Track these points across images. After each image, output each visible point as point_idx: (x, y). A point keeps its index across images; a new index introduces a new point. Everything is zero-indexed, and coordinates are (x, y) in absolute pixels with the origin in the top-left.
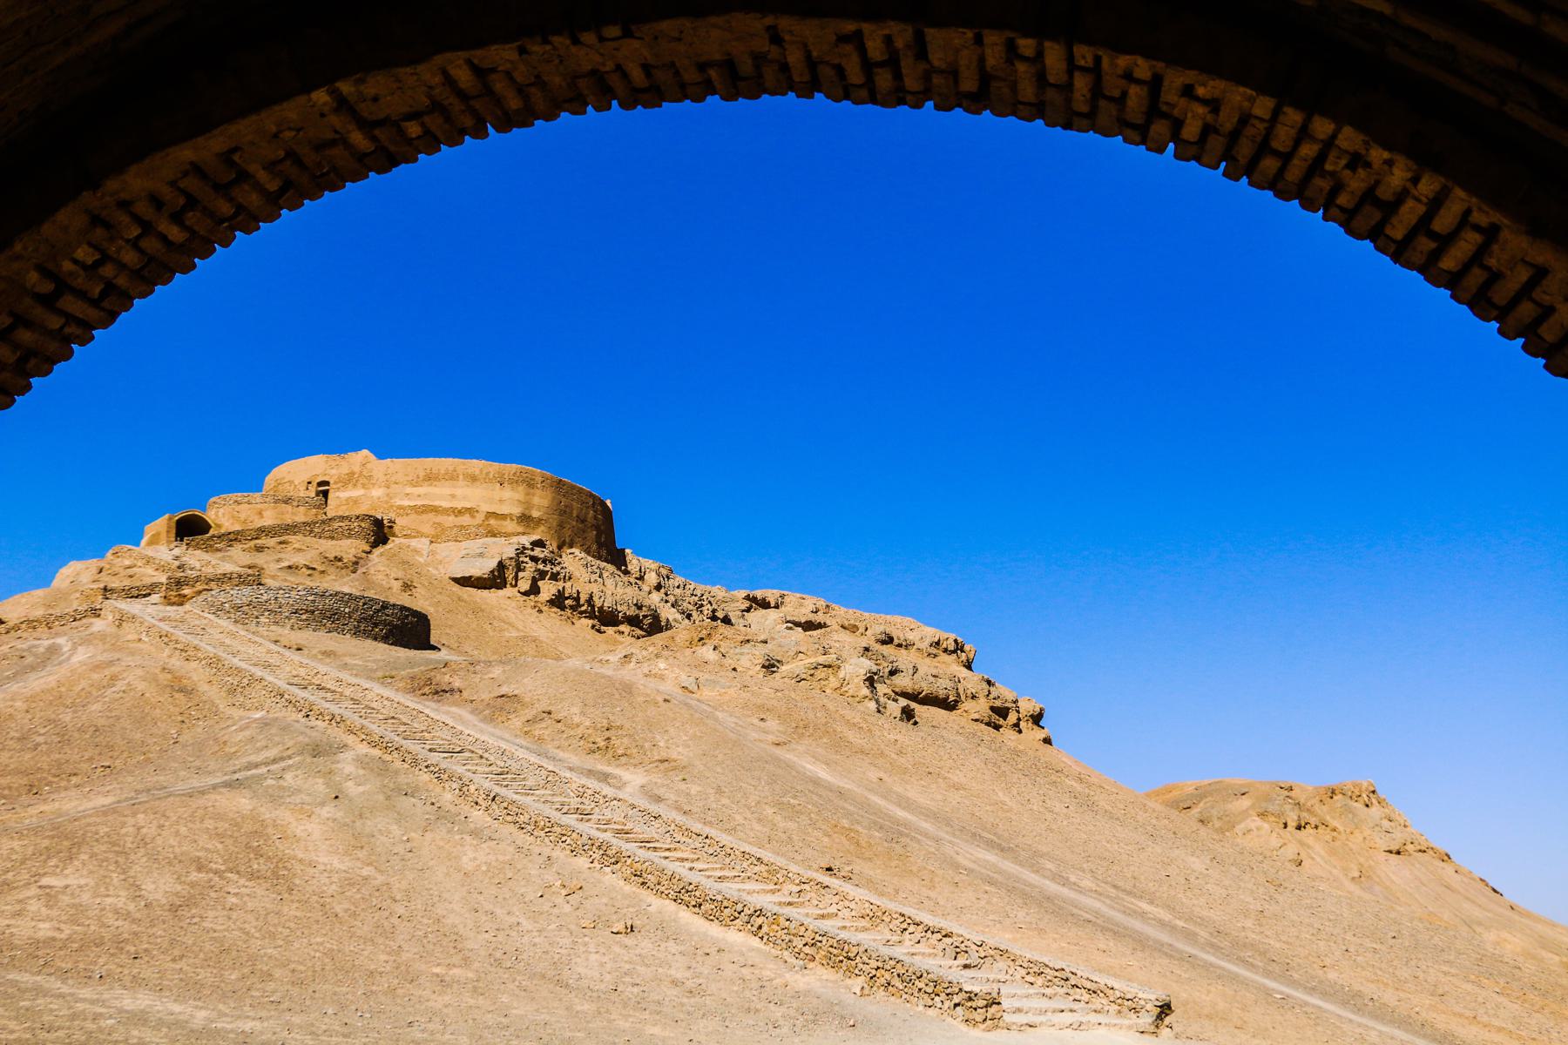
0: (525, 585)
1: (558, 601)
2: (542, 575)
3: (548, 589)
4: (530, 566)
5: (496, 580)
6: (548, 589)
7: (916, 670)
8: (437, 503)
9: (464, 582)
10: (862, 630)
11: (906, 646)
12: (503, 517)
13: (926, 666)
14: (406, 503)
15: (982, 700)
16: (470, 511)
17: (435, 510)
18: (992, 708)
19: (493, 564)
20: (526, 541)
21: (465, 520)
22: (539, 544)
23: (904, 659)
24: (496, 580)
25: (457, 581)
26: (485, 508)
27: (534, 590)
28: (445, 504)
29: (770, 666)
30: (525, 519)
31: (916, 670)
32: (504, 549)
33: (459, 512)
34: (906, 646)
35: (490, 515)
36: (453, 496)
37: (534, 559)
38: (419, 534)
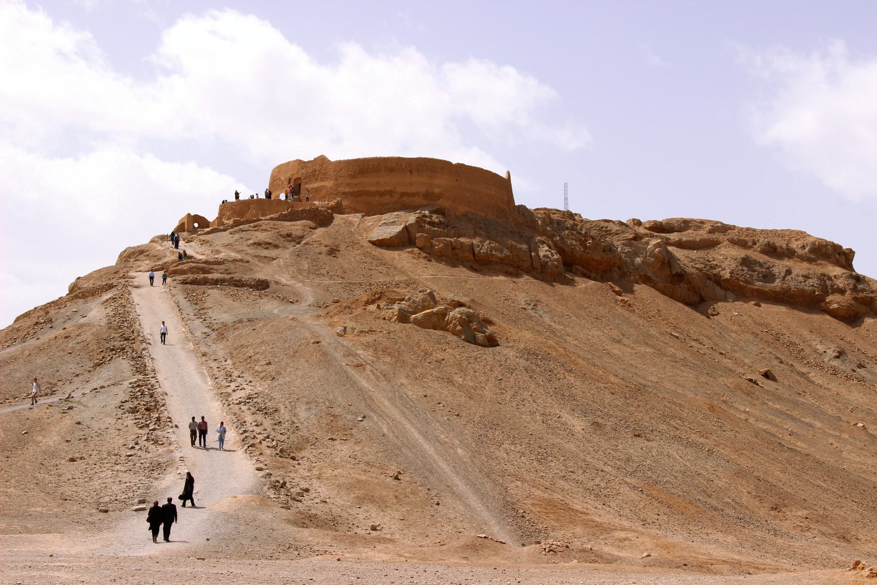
7: (789, 272)
8: (367, 189)
9: (381, 244)
10: (750, 244)
11: (789, 253)
12: (413, 195)
13: (799, 268)
14: (347, 190)
15: (848, 292)
16: (391, 193)
17: (368, 193)
18: (855, 299)
19: (399, 228)
21: (387, 199)
23: (779, 266)
25: (374, 243)
26: (399, 189)
28: (373, 189)
31: (789, 272)
33: (382, 194)
34: (789, 253)
35: (403, 194)
36: (378, 183)
37: (430, 223)
38: (356, 211)
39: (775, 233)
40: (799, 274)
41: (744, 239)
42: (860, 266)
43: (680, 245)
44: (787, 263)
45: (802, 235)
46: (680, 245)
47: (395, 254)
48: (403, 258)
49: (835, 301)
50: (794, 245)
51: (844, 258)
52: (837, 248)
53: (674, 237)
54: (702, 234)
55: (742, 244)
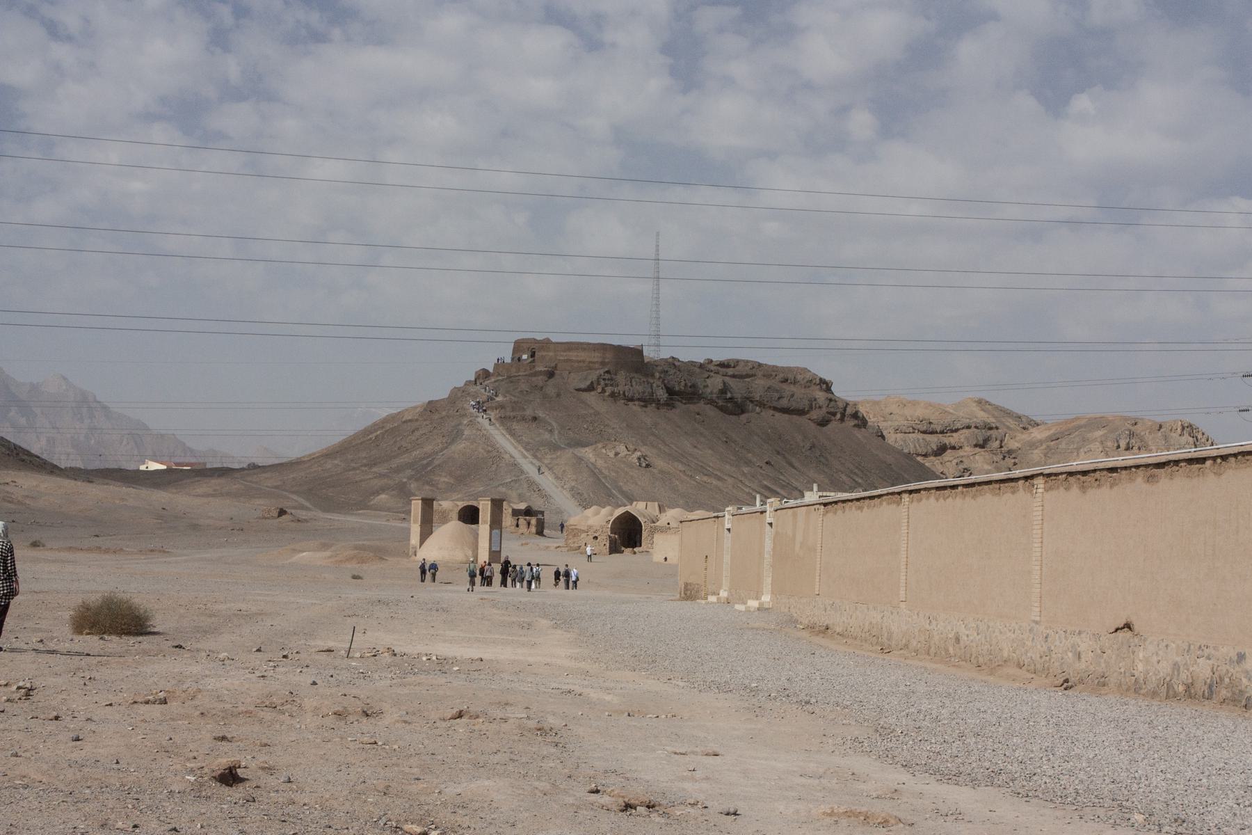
0: (599, 390)
1: (613, 395)
2: (606, 385)
3: (609, 390)
4: (602, 383)
5: (591, 388)
6: (609, 390)
7: (792, 396)
11: (795, 382)
19: (588, 383)
20: (602, 372)
22: (608, 372)
23: (788, 389)
24: (591, 388)
27: (603, 391)
29: (617, 454)
30: (603, 364)
32: (593, 376)
34: (795, 382)
39: (790, 369)
40: (799, 395)
41: (769, 372)
42: (839, 391)
43: (734, 376)
44: (792, 388)
45: (805, 370)
46: (734, 376)
47: (585, 395)
48: (591, 397)
49: (815, 414)
50: (799, 377)
51: (826, 386)
52: (822, 381)
53: (730, 371)
54: (746, 370)
55: (767, 376)
